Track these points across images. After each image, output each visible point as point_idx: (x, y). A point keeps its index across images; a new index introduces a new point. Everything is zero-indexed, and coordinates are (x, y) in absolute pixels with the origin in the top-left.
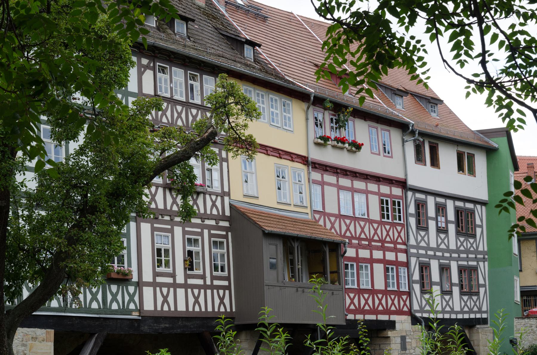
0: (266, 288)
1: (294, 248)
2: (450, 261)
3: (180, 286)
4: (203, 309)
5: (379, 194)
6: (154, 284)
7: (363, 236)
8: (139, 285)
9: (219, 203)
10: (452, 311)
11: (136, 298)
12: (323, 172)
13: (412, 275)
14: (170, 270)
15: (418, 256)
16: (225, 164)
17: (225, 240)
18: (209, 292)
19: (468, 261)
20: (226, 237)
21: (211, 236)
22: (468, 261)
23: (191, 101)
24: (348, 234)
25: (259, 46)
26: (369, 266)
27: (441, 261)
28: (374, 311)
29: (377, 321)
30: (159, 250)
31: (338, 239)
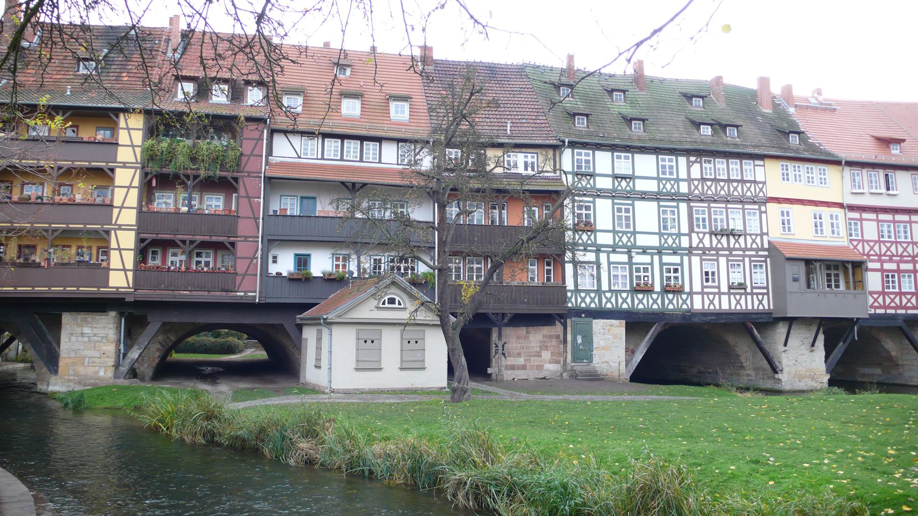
0: (788, 295)
3: (724, 294)
4: (744, 308)
6: (702, 293)
8: (691, 294)
9: (758, 240)
11: (688, 302)
14: (716, 284)
16: (764, 215)
17: (764, 264)
18: (749, 297)
20: (765, 261)
21: (751, 261)
23: (731, 178)
24: (889, 253)
25: (803, 133)
26: (912, 275)
30: (707, 273)
31: (857, 258)
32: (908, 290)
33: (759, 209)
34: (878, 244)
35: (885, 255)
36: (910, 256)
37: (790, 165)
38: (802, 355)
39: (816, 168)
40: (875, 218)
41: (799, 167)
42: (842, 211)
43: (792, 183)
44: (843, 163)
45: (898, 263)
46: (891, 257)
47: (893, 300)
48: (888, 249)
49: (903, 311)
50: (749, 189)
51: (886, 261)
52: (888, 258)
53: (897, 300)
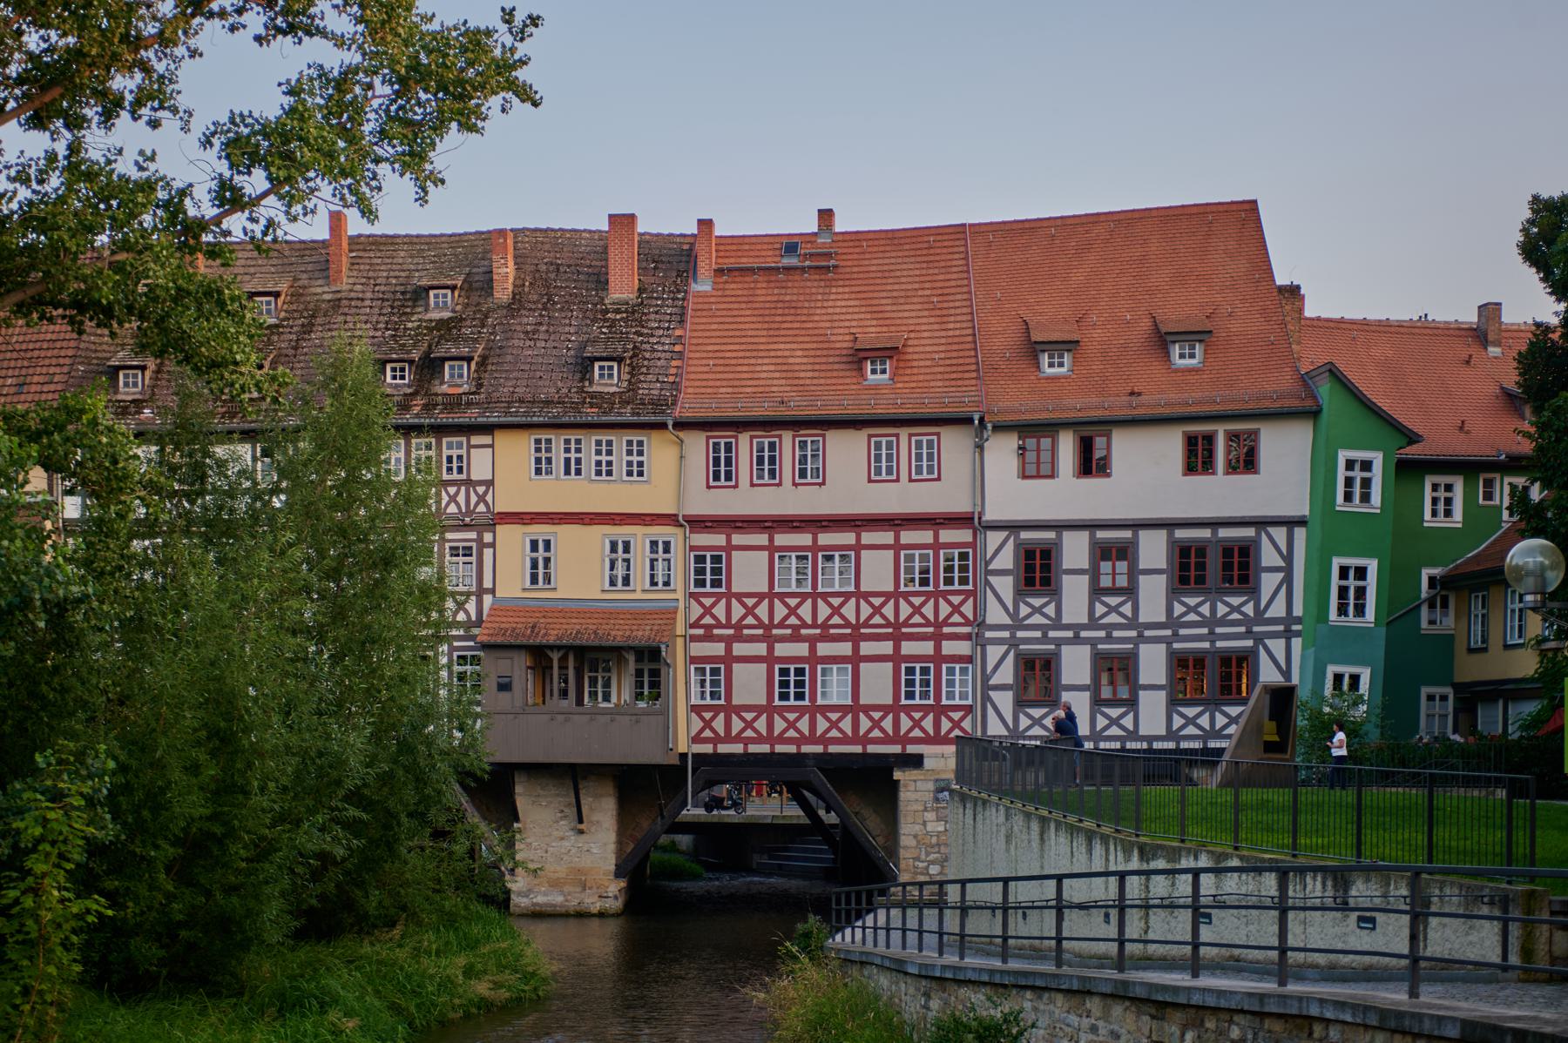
1: (551, 660)
2: (1137, 645)
5: (897, 547)
7: (836, 620)
9: (471, 606)
10: (1134, 735)
12: (730, 530)
13: (986, 678)
15: (1013, 643)
16: (488, 552)
19: (1213, 642)
22: (1213, 642)
24: (793, 620)
27: (1100, 646)
28: (855, 739)
29: (865, 755)
32: (834, 701)
33: (479, 540)
34: (766, 601)
35: (781, 625)
36: (848, 624)
37: (558, 440)
38: (562, 839)
39: (620, 440)
40: (766, 543)
41: (578, 442)
42: (679, 531)
43: (557, 479)
44: (670, 427)
45: (813, 641)
46: (795, 628)
47: (792, 725)
48: (793, 611)
49: (819, 749)
50: (453, 499)
51: (783, 639)
52: (789, 631)
53: (804, 725)
